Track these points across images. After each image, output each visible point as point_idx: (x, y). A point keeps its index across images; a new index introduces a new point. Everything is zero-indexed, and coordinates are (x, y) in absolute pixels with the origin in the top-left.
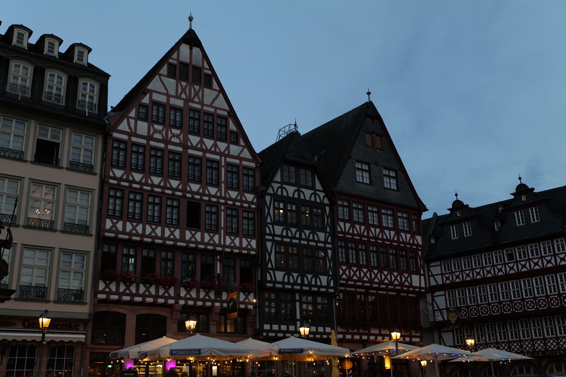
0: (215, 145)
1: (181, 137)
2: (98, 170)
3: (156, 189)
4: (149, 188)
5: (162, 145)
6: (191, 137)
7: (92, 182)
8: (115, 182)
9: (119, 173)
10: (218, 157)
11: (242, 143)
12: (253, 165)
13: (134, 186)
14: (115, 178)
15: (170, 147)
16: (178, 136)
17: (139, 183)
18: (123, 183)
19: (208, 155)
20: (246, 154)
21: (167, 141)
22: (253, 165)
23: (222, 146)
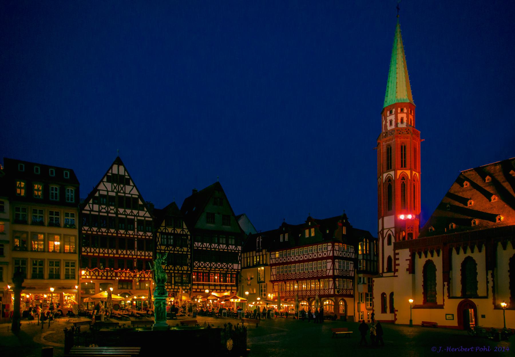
0: (132, 212)
1: (115, 210)
2: (77, 227)
3: (104, 234)
4: (101, 233)
5: (106, 214)
6: (119, 209)
7: (76, 232)
8: (85, 232)
9: (86, 228)
10: (133, 217)
11: (145, 210)
12: (151, 219)
13: (94, 233)
14: (84, 230)
15: (110, 215)
16: (113, 210)
17: (96, 231)
18: (89, 232)
19: (128, 217)
20: (148, 214)
21: (108, 212)
22: (151, 219)
23: (135, 212)
